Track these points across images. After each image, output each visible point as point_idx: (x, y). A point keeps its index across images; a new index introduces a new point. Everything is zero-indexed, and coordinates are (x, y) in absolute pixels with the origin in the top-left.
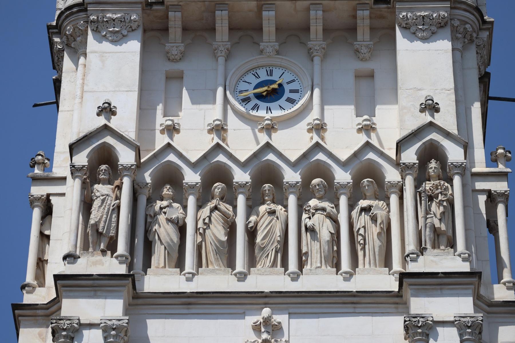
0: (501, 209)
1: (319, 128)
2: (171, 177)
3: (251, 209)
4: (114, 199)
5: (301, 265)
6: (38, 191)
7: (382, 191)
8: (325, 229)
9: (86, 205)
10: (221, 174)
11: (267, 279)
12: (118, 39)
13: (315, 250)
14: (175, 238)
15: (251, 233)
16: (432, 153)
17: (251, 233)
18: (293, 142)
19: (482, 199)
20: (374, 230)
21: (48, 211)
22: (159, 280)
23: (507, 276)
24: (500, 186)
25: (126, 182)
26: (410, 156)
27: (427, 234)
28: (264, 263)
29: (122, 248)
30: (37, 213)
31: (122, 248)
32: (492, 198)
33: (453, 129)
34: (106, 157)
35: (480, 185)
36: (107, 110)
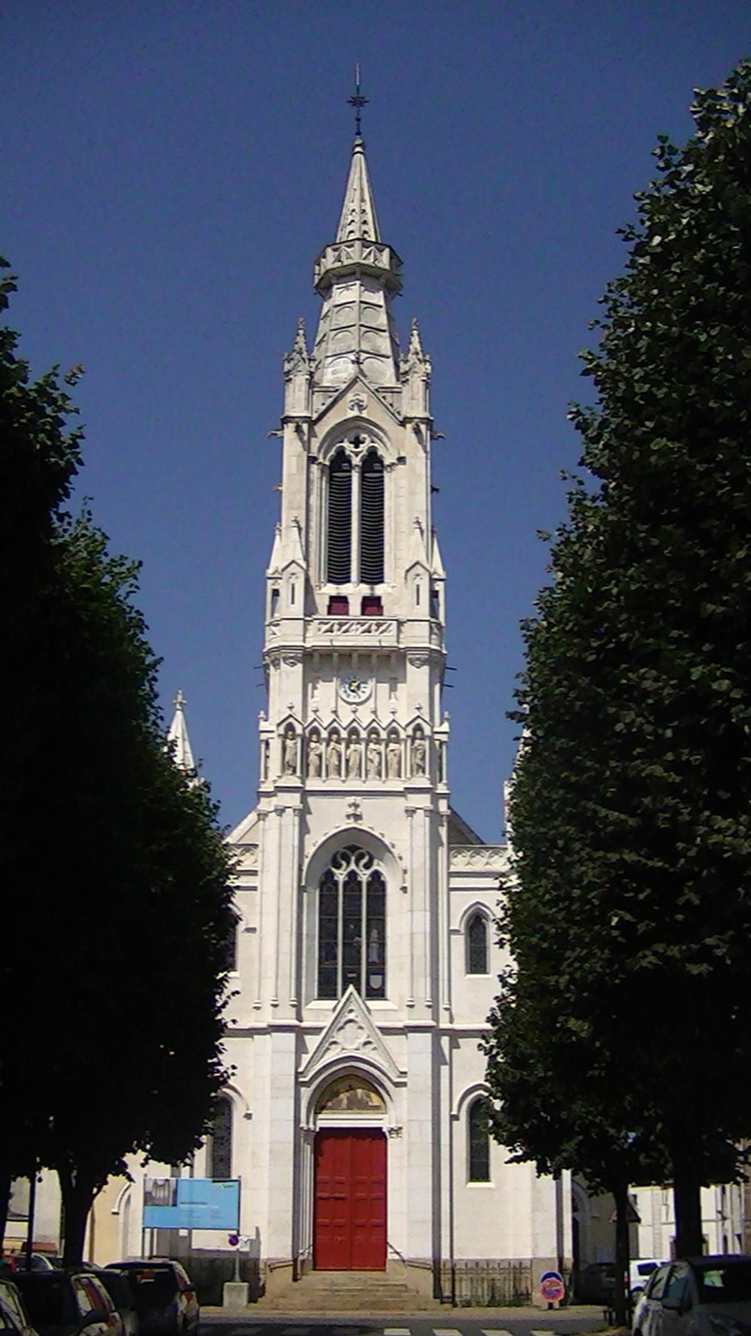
0: (444, 747)
1: (374, 712)
2: (315, 731)
3: (347, 747)
4: (294, 745)
5: (366, 775)
6: (264, 736)
7: (398, 741)
8: (376, 760)
9: (284, 749)
10: (335, 731)
11: (354, 784)
12: (293, 664)
13: (372, 768)
14: (317, 762)
15: (347, 761)
16: (418, 728)
17: (347, 761)
18: (365, 717)
19: (437, 743)
20: (396, 760)
21: (267, 744)
22: (313, 784)
23: (444, 781)
24: (444, 738)
25: (299, 740)
26: (410, 731)
27: (415, 767)
28: (352, 775)
29: (298, 773)
30: (263, 746)
31: (298, 773)
32: (442, 743)
33: (427, 719)
34: (290, 727)
35: (437, 736)
36: (291, 708)
